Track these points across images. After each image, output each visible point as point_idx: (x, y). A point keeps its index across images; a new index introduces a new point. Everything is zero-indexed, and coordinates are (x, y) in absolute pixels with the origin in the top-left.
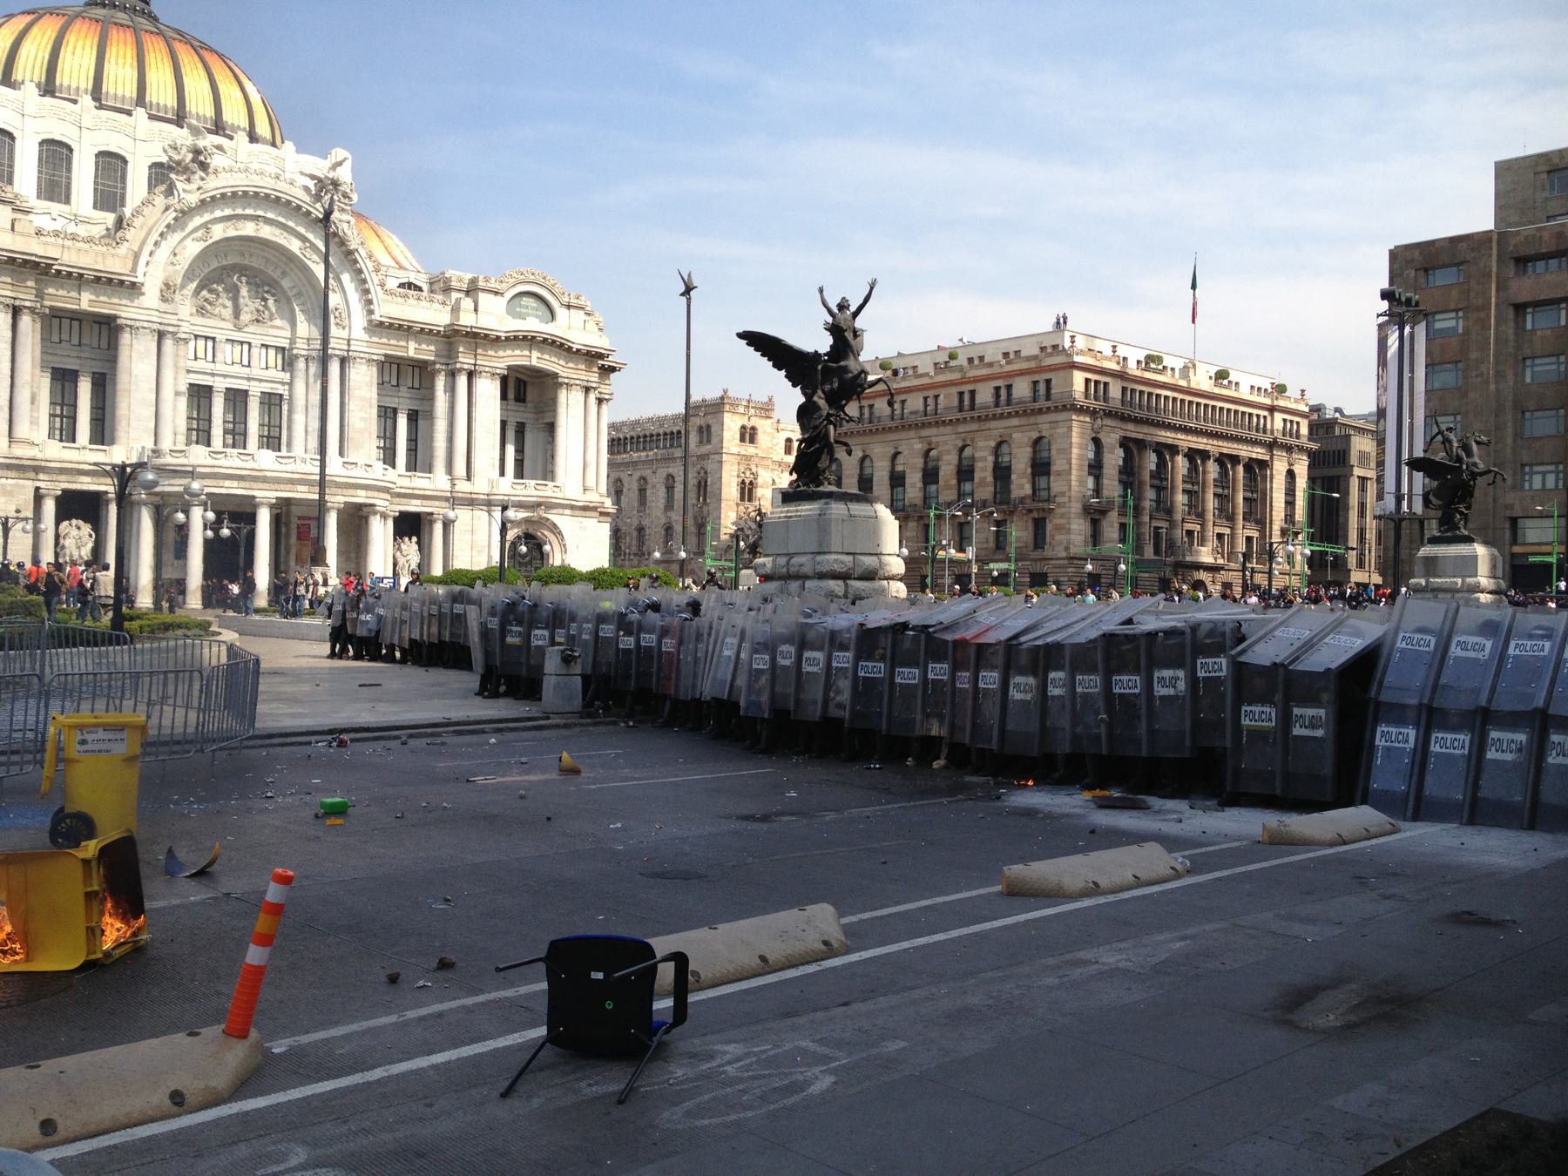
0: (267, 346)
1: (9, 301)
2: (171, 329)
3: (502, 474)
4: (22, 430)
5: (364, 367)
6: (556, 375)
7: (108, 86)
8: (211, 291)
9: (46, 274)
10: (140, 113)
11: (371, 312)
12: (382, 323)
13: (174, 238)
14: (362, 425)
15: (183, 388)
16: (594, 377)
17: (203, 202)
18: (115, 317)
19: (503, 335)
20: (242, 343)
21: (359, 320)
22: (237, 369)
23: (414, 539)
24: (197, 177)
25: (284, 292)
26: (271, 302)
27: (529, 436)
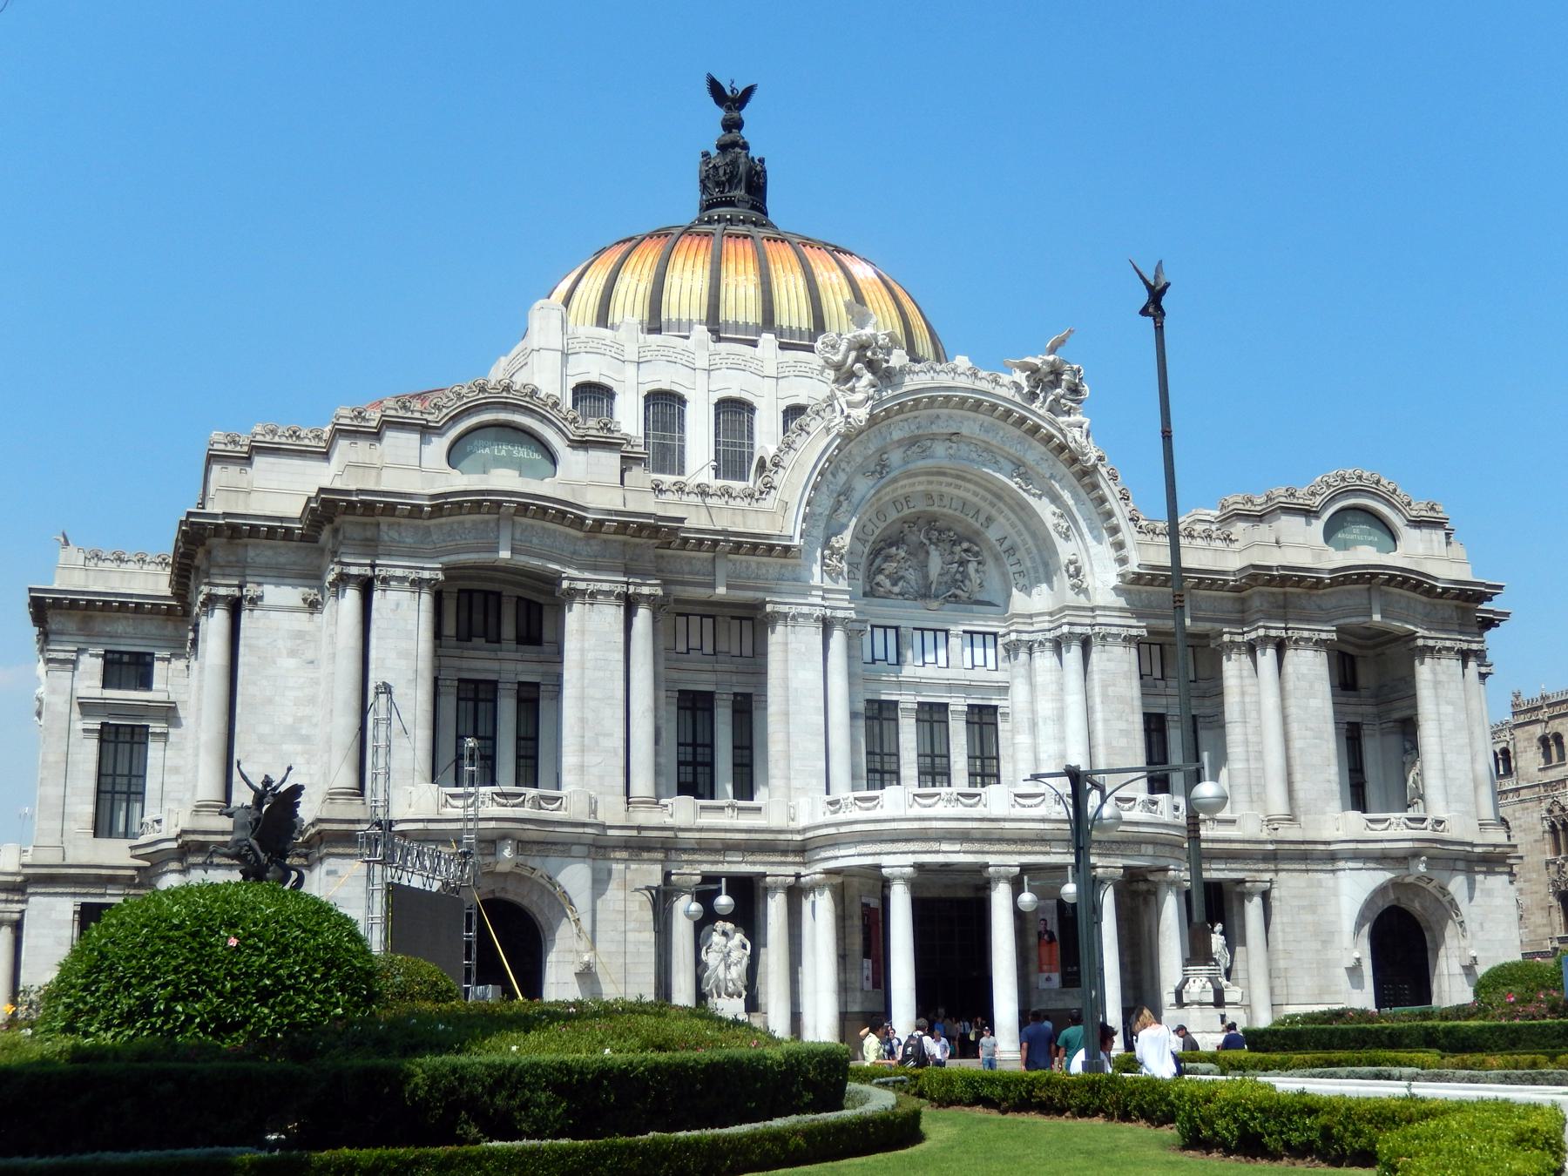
1: (619, 589)
2: (840, 614)
7: (728, 313)
8: (888, 558)
9: (668, 546)
10: (768, 340)
11: (1123, 561)
15: (861, 707)
17: (873, 420)
21: (1104, 579)
23: (1219, 927)
25: (991, 548)
26: (972, 567)
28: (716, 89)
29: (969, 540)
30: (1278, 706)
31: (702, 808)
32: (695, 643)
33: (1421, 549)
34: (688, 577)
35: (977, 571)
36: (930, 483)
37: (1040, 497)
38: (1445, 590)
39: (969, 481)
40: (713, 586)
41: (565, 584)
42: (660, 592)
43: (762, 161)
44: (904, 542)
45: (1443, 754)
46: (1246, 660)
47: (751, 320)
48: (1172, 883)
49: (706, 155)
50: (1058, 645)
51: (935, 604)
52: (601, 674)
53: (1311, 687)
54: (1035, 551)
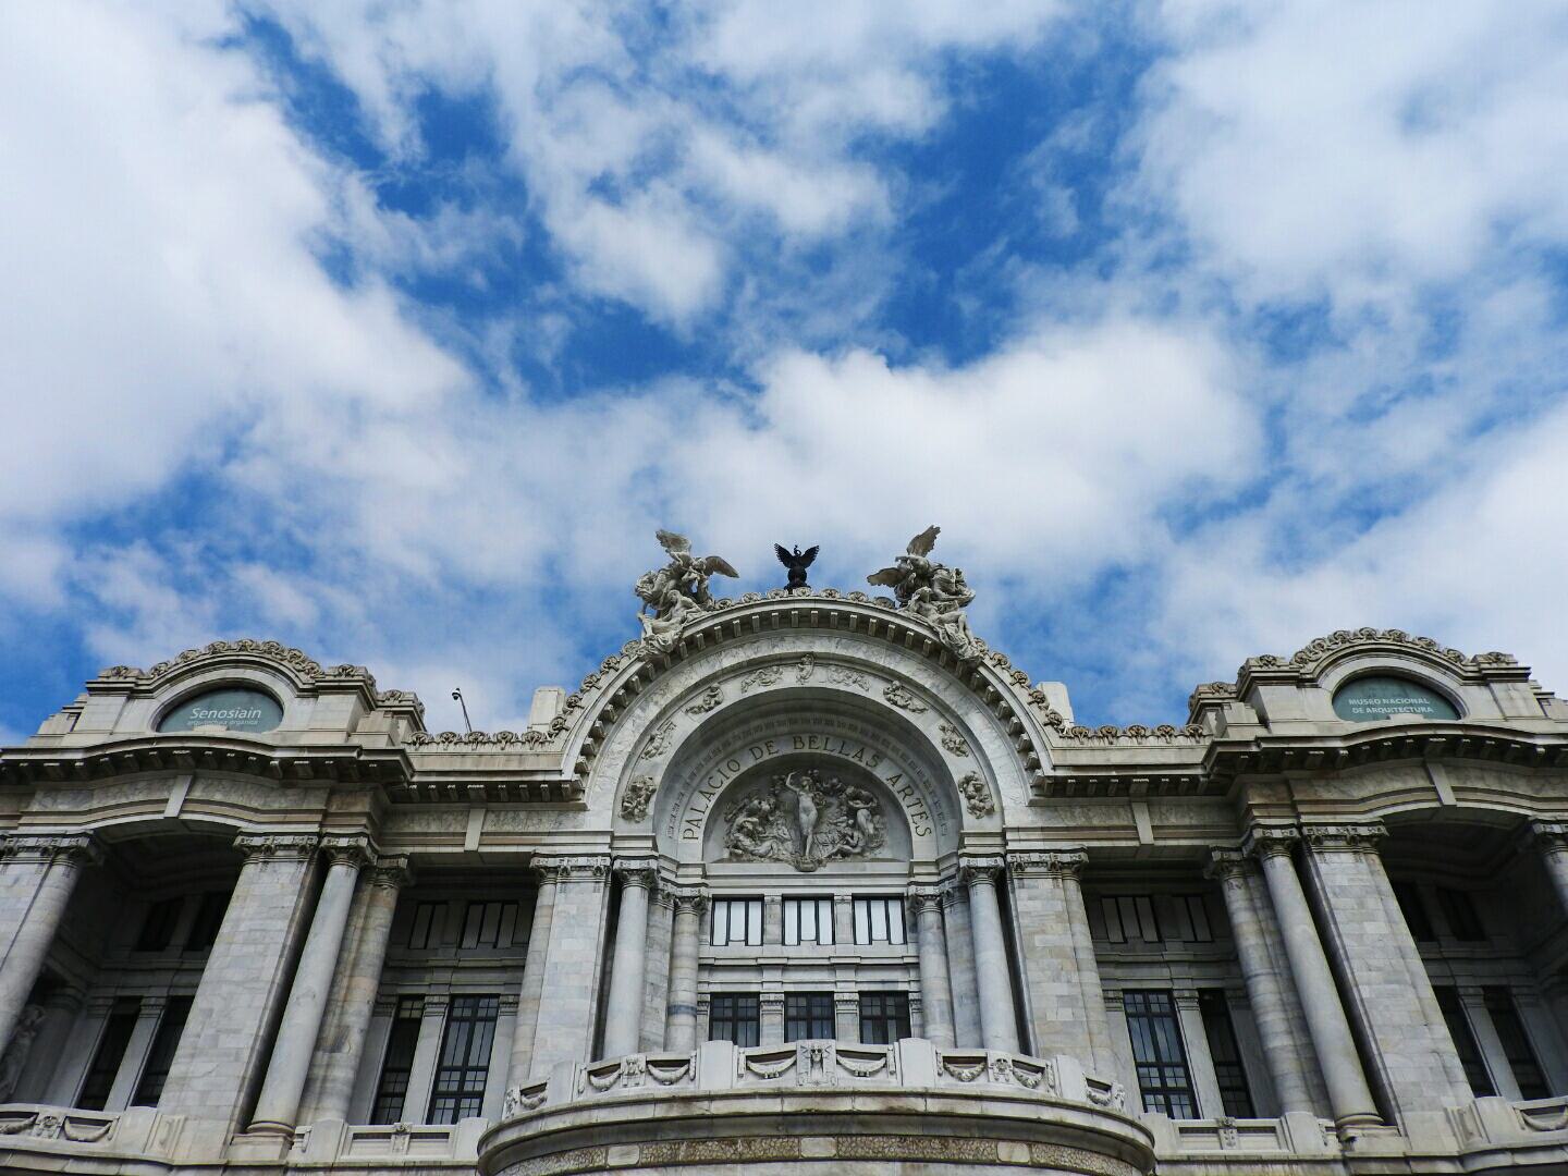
0: (869, 898)
2: (635, 865)
3: (1482, 1085)
4: (276, 1103)
5: (1046, 884)
6: (1524, 823)
11: (1035, 765)
12: (1055, 777)
13: (643, 714)
14: (1066, 1014)
15: (685, 994)
20: (817, 899)
21: (1014, 797)
22: (807, 952)
24: (678, 605)
26: (862, 815)
27: (1534, 1022)
28: (783, 554)
29: (857, 787)
31: (357, 1136)
32: (488, 935)
35: (872, 821)
36: (793, 722)
37: (922, 711)
39: (844, 713)
40: (463, 845)
41: (238, 840)
42: (363, 842)
44: (776, 796)
46: (1253, 882)
50: (963, 893)
52: (252, 949)
53: (1361, 905)
54: (933, 782)
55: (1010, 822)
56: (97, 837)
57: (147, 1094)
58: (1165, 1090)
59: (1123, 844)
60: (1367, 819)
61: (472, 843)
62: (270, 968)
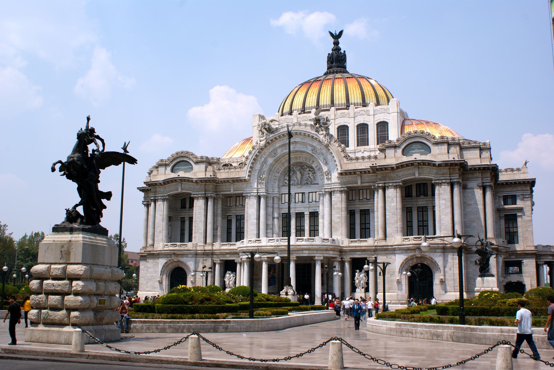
2: (262, 194)
7: (307, 105)
14: (338, 220)
15: (276, 215)
16: (456, 178)
17: (268, 143)
18: (243, 194)
19: (394, 166)
26: (311, 174)
28: (331, 34)
30: (388, 206)
33: (438, 152)
34: (225, 190)
38: (440, 165)
40: (230, 191)
42: (213, 195)
43: (344, 51)
45: (440, 216)
47: (313, 106)
48: (318, 260)
49: (329, 54)
51: (299, 186)
53: (392, 200)
55: (333, 181)
56: (169, 195)
57: (190, 240)
58: (365, 229)
59: (355, 185)
60: (399, 182)
61: (232, 192)
62: (203, 218)
